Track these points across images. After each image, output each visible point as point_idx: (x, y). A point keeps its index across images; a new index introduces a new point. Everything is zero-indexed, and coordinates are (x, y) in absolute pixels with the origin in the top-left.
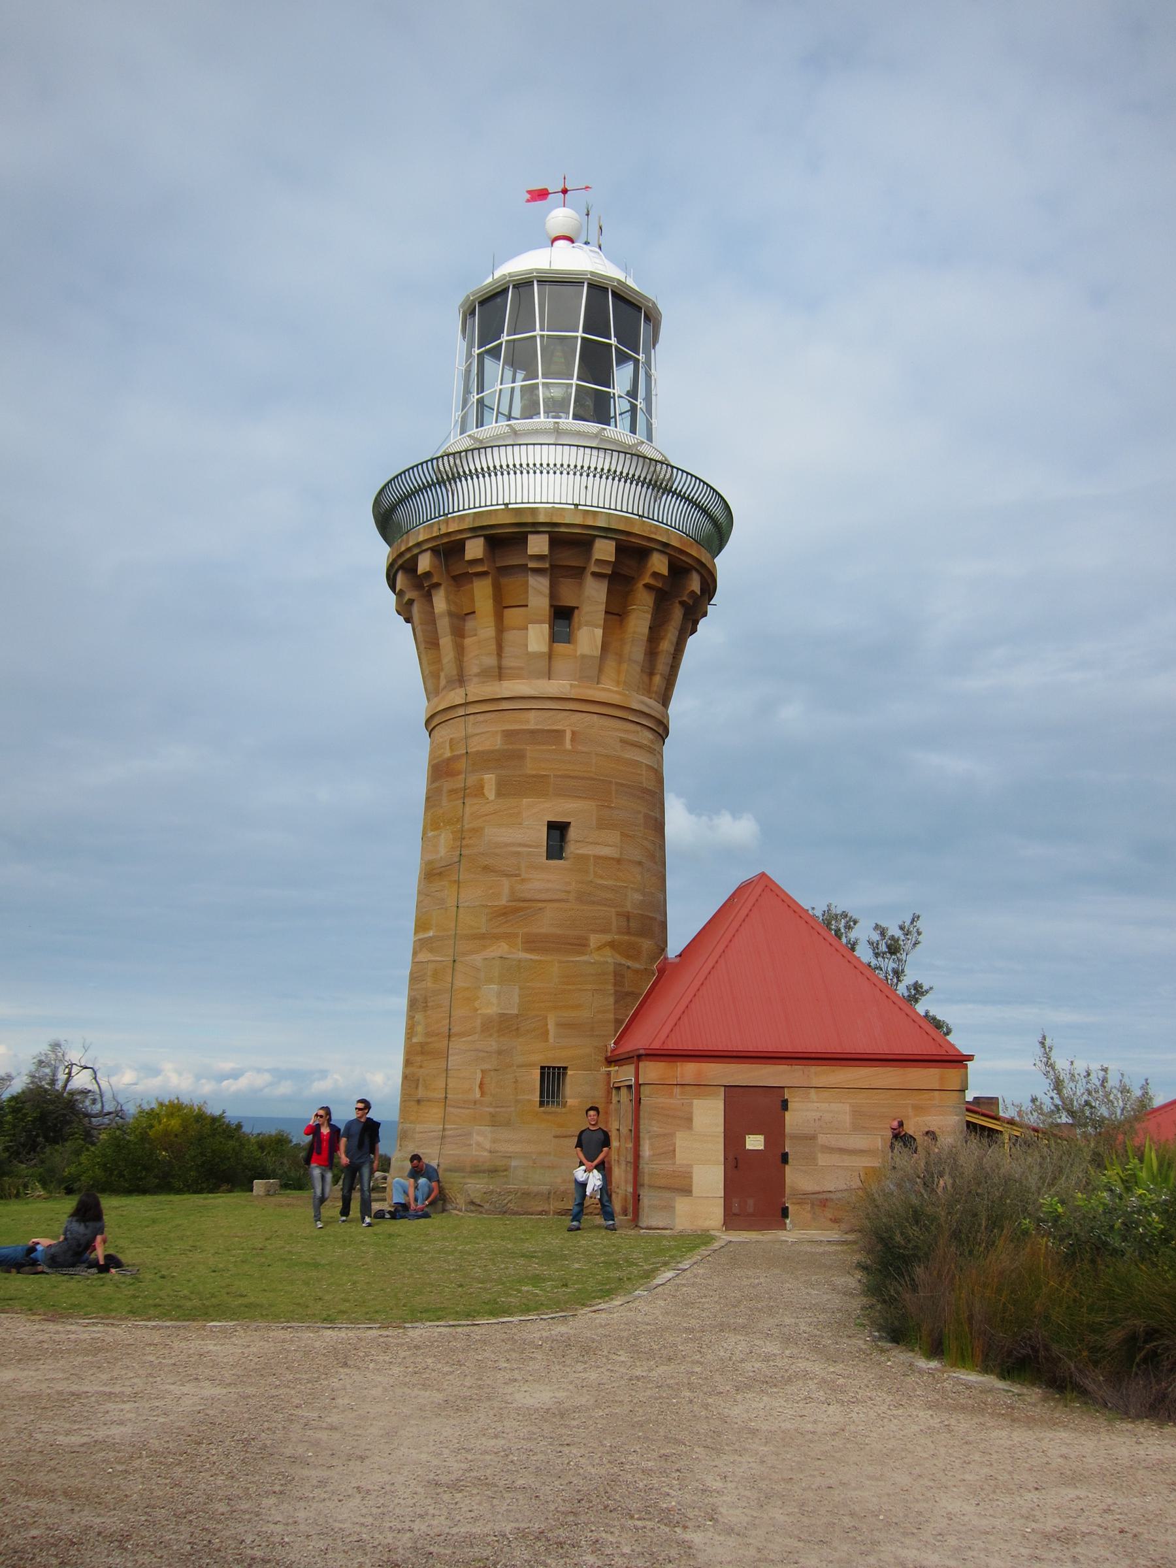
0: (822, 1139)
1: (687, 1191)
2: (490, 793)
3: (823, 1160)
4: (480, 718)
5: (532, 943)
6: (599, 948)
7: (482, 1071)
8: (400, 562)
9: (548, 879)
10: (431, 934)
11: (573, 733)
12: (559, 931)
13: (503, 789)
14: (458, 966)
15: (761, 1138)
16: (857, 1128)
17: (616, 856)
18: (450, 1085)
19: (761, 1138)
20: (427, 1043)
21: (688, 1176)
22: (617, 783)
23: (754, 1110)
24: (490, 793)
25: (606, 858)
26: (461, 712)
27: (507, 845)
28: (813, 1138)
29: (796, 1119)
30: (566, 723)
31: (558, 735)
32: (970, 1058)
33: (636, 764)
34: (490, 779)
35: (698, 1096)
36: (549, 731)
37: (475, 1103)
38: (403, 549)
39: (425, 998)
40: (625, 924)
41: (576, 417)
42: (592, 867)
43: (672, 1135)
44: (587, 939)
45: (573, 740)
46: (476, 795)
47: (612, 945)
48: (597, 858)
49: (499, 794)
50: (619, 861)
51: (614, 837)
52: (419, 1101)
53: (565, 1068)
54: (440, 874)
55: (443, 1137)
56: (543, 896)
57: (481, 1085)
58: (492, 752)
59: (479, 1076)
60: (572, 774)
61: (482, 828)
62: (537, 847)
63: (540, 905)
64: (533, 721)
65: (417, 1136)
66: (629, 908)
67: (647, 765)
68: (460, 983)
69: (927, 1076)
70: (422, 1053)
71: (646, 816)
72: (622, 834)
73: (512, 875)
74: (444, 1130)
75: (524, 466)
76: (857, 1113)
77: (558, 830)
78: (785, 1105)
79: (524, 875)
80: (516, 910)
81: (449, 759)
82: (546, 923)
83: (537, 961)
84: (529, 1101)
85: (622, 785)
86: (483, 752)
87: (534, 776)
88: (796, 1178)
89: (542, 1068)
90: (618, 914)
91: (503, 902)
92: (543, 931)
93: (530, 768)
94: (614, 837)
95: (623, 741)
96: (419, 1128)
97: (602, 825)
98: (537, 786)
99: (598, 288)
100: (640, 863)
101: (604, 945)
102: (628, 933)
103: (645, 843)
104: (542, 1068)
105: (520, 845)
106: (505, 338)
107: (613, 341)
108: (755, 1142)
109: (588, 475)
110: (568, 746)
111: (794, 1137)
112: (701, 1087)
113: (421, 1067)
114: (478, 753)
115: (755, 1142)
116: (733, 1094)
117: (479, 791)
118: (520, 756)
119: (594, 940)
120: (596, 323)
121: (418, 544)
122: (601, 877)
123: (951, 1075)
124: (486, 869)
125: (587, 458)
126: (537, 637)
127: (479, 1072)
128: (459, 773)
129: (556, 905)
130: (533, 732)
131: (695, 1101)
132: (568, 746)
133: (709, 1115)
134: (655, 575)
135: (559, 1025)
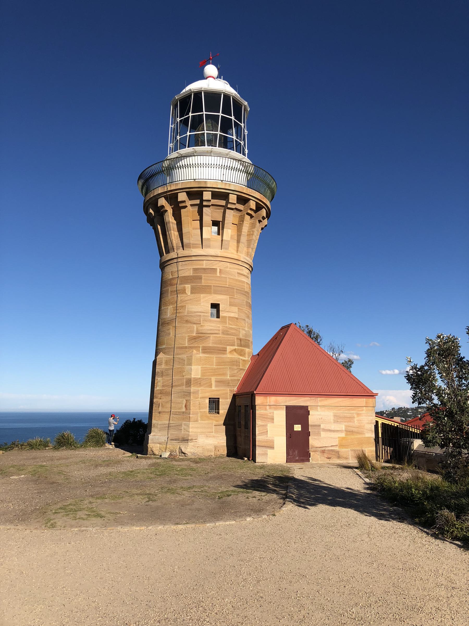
0: (322, 426)
1: (272, 448)
2: (188, 291)
3: (323, 434)
5: (206, 350)
6: (230, 352)
8: (150, 201)
9: (211, 325)
10: (164, 347)
11: (220, 270)
13: (193, 291)
15: (300, 426)
16: (336, 422)
17: (237, 317)
18: (173, 406)
19: (300, 426)
21: (273, 442)
22: (236, 289)
23: (297, 415)
24: (188, 291)
26: (175, 261)
27: (195, 312)
28: (320, 426)
29: (313, 418)
31: (215, 269)
32: (377, 394)
33: (243, 282)
34: (188, 287)
35: (276, 409)
36: (210, 269)
37: (183, 413)
38: (152, 196)
40: (239, 342)
41: (220, 146)
43: (267, 425)
44: (226, 348)
45: (220, 272)
46: (182, 293)
47: (235, 350)
48: (229, 317)
49: (192, 293)
50: (237, 318)
51: (235, 309)
52: (160, 413)
53: (219, 399)
54: (168, 323)
56: (209, 332)
58: (188, 276)
59: (184, 402)
61: (185, 306)
62: (206, 313)
64: (205, 265)
65: (159, 426)
66: (241, 337)
69: (362, 401)
71: (247, 302)
72: (238, 309)
73: (197, 324)
75: (197, 167)
76: (335, 416)
77: (215, 306)
78: (308, 413)
80: (199, 337)
81: (171, 279)
82: (210, 343)
83: (207, 357)
84: (205, 412)
86: (185, 276)
88: (313, 441)
89: (210, 398)
90: (237, 339)
91: (195, 335)
93: (204, 283)
94: (235, 309)
95: (238, 273)
97: (231, 304)
98: (206, 290)
99: (227, 97)
101: (232, 351)
102: (241, 346)
104: (210, 398)
105: (200, 312)
106: (190, 114)
107: (233, 118)
108: (298, 428)
109: (226, 169)
110: (218, 274)
111: (311, 426)
112: (276, 406)
113: (160, 399)
114: (182, 277)
115: (298, 428)
116: (289, 409)
117: (184, 291)
118: (200, 278)
119: (229, 348)
120: (226, 110)
121: (159, 195)
123: (370, 400)
124: (187, 322)
125: (229, 162)
127: (185, 400)
130: (204, 269)
131: (275, 412)
132: (218, 274)
133: (281, 417)
134: (251, 209)
135: (216, 381)
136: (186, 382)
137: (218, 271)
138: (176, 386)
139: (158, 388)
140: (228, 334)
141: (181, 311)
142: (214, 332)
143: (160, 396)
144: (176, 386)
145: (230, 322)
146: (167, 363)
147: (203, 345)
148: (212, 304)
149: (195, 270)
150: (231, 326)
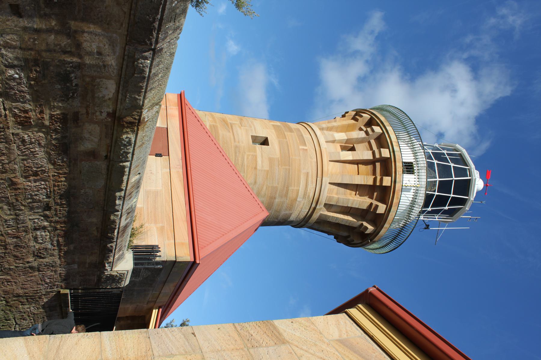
11: (306, 150)
12: (220, 137)
17: (259, 167)
25: (256, 161)
30: (309, 147)
31: (305, 144)
42: (251, 153)
45: (303, 149)
50: (256, 168)
51: (266, 167)
56: (234, 131)
60: (290, 148)
63: (231, 131)
67: (299, 190)
72: (268, 171)
77: (265, 142)
78: (158, 155)
79: (242, 128)
80: (227, 124)
85: (289, 172)
87: (285, 135)
92: (220, 132)
94: (266, 167)
95: (308, 173)
97: (271, 160)
100: (255, 182)
103: (265, 188)
122: (247, 158)
126: (342, 136)
129: (232, 137)
132: (301, 147)
137: (305, 148)
140: (236, 153)
142: (236, 136)
145: (250, 157)
147: (219, 126)
148: (267, 138)
150: (246, 157)
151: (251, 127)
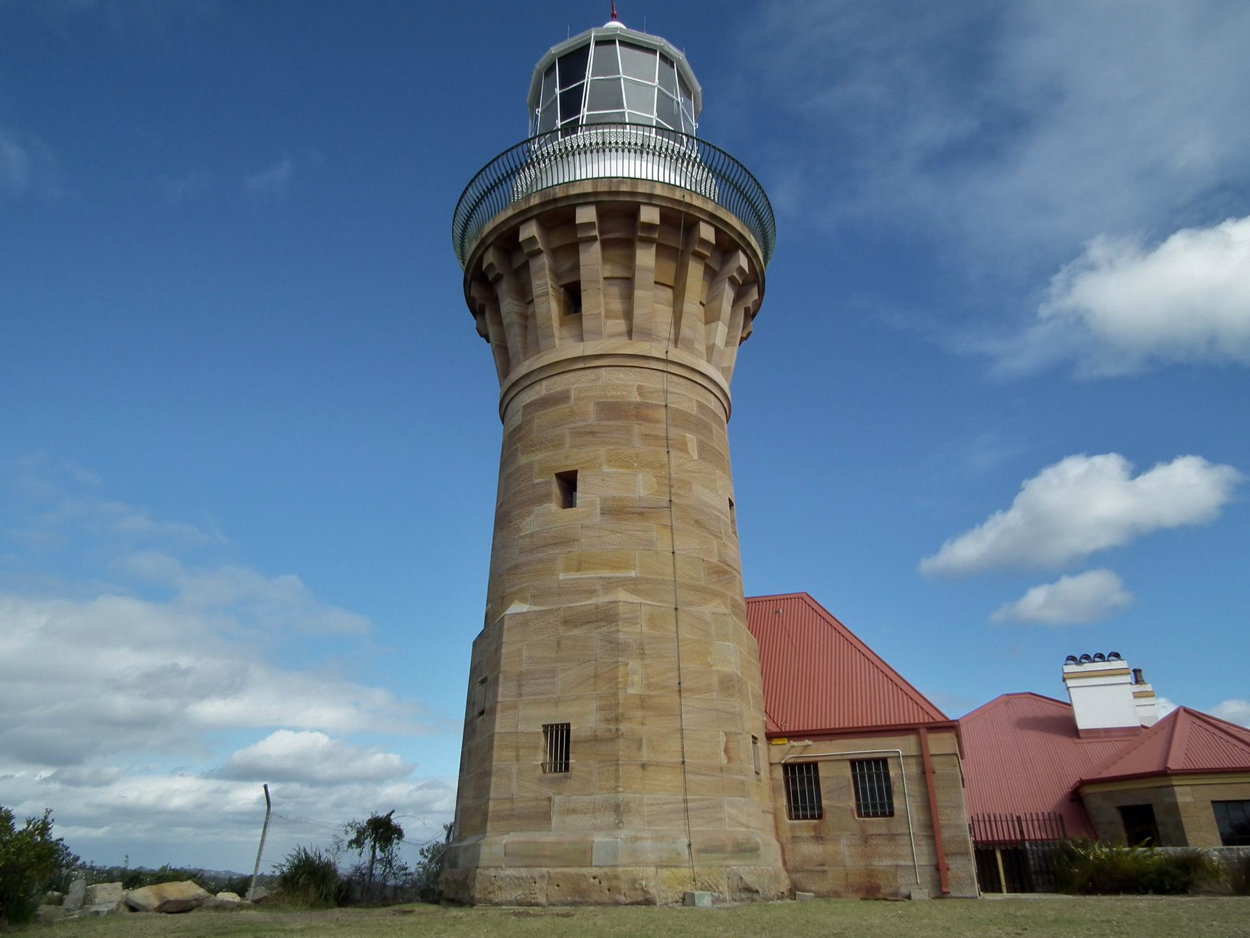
4: (675, 379)
7: (726, 734)
10: (633, 574)
14: (681, 615)
20: (649, 696)
26: (654, 365)
39: (641, 644)
46: (680, 449)
49: (700, 456)
52: (643, 766)
54: (641, 514)
55: (686, 810)
57: (726, 750)
59: (723, 739)
68: (684, 634)
70: (643, 707)
74: (686, 801)
80: (725, 572)
96: (647, 798)
113: (643, 724)
114: (677, 410)
117: (683, 447)
127: (721, 734)
128: (656, 421)
136: (721, 683)
138: (691, 690)
139: (630, 691)
141: (681, 492)
143: (639, 713)
144: (691, 690)
146: (652, 619)
149: (701, 406)
151: (719, 518)
